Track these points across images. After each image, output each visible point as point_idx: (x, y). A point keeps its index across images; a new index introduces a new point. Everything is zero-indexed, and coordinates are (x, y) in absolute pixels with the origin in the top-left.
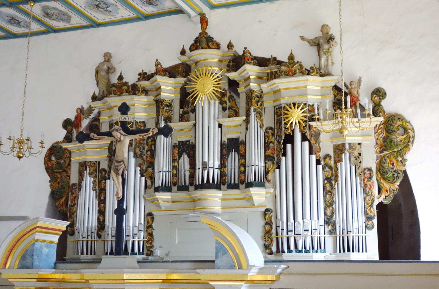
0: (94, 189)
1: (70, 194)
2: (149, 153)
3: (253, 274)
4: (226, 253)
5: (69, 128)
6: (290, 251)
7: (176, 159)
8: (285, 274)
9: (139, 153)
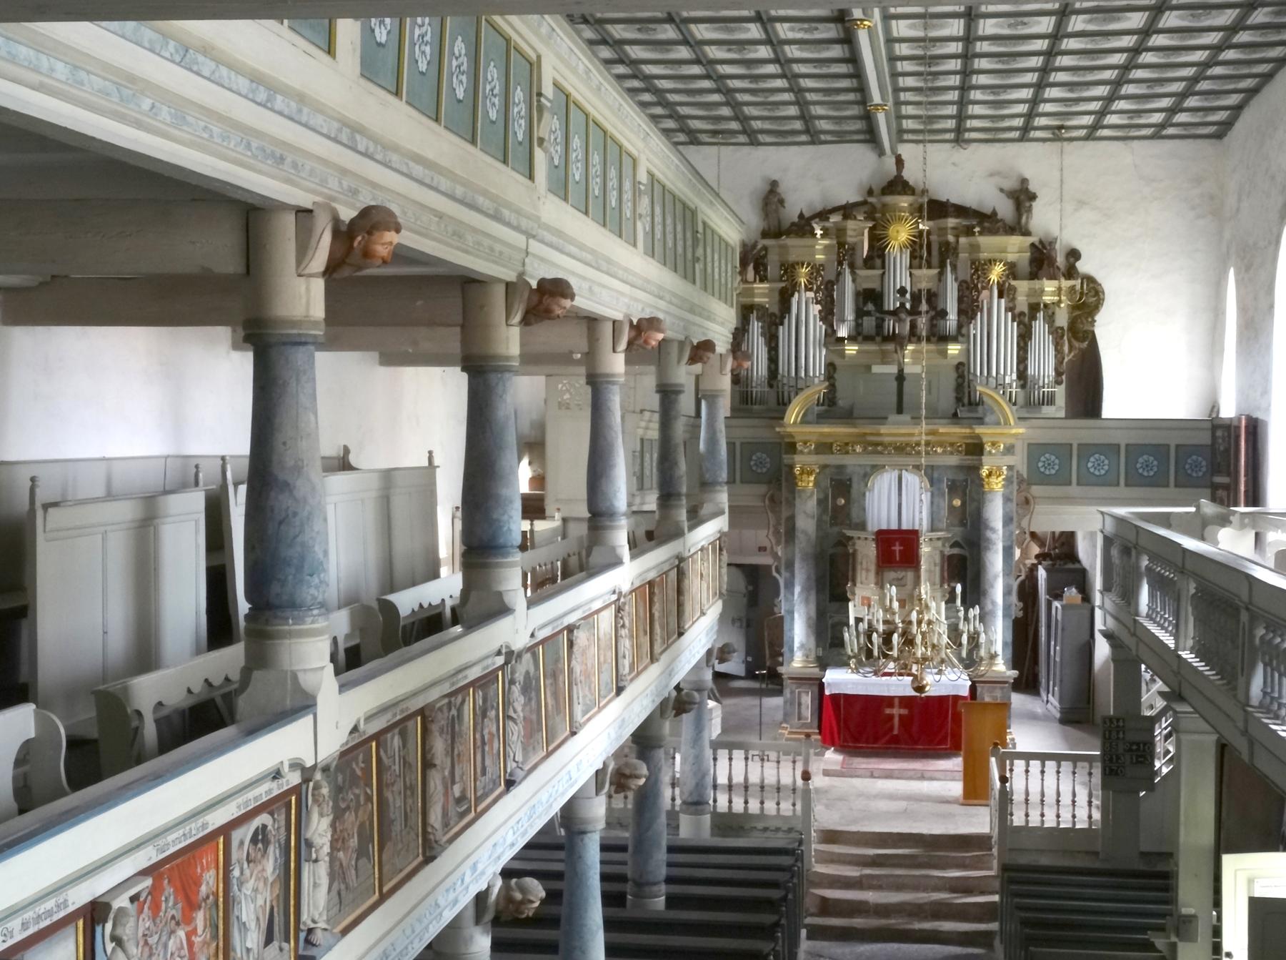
0: (763, 334)
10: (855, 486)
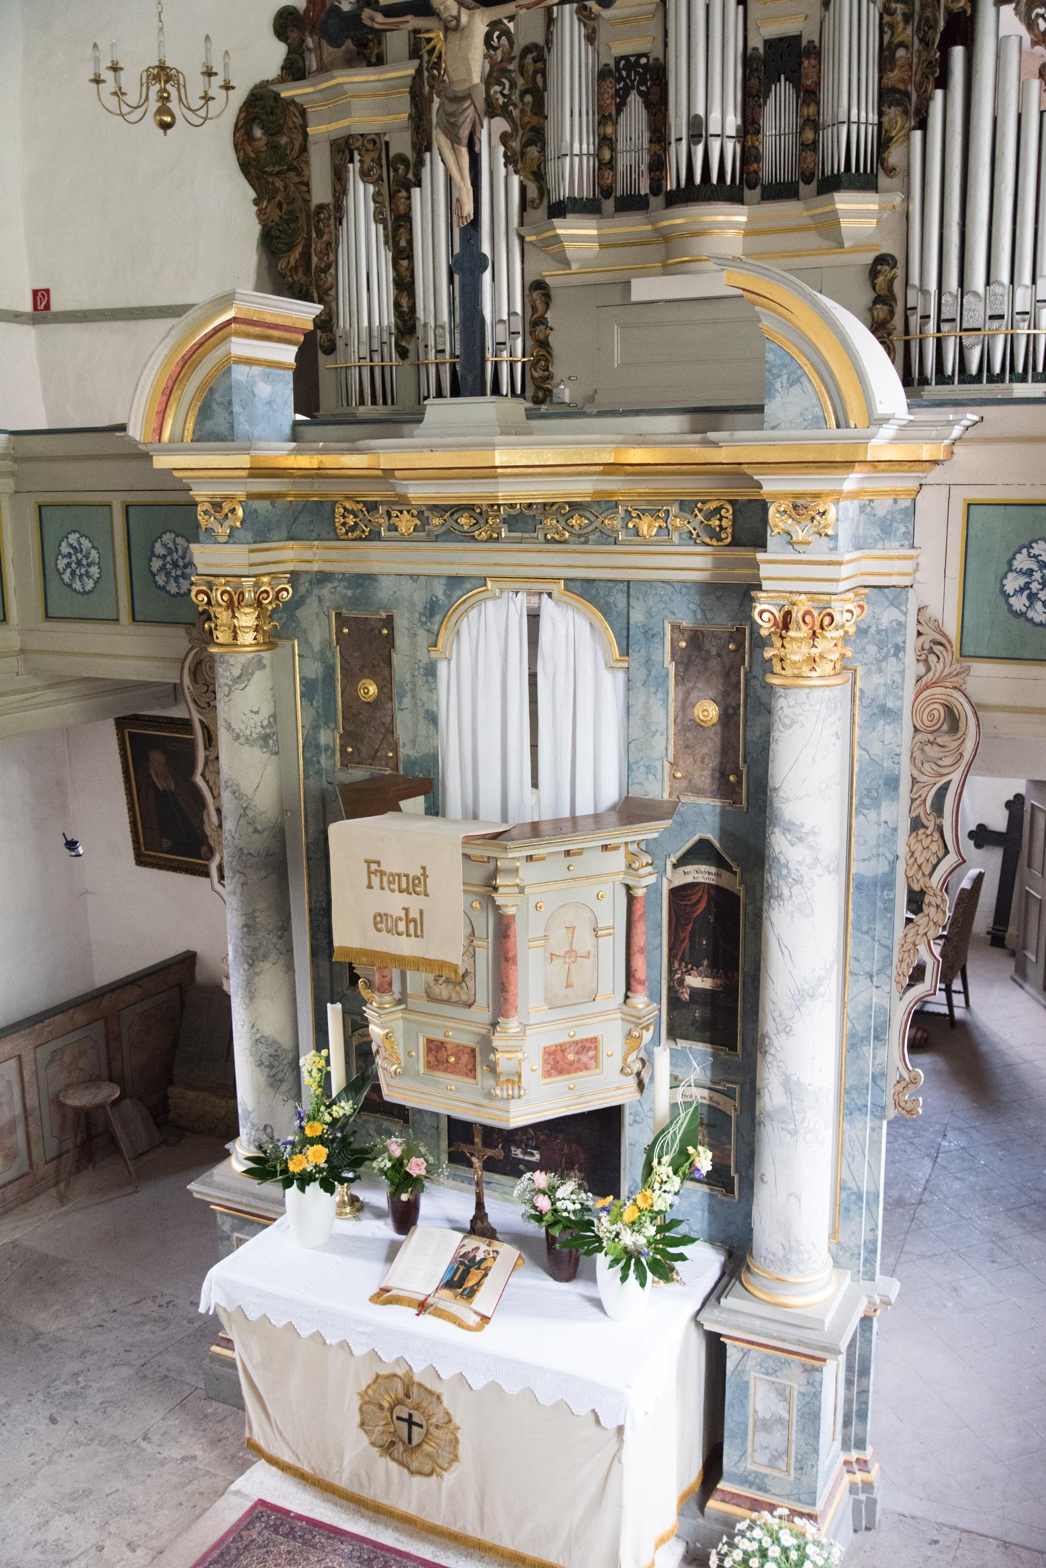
1: (314, 235)
2: (528, 98)
3: (882, 445)
4: (798, 380)
5: (294, 35)
6: (942, 379)
7: (610, 115)
8: (972, 440)
9: (501, 101)
10: (402, 642)
